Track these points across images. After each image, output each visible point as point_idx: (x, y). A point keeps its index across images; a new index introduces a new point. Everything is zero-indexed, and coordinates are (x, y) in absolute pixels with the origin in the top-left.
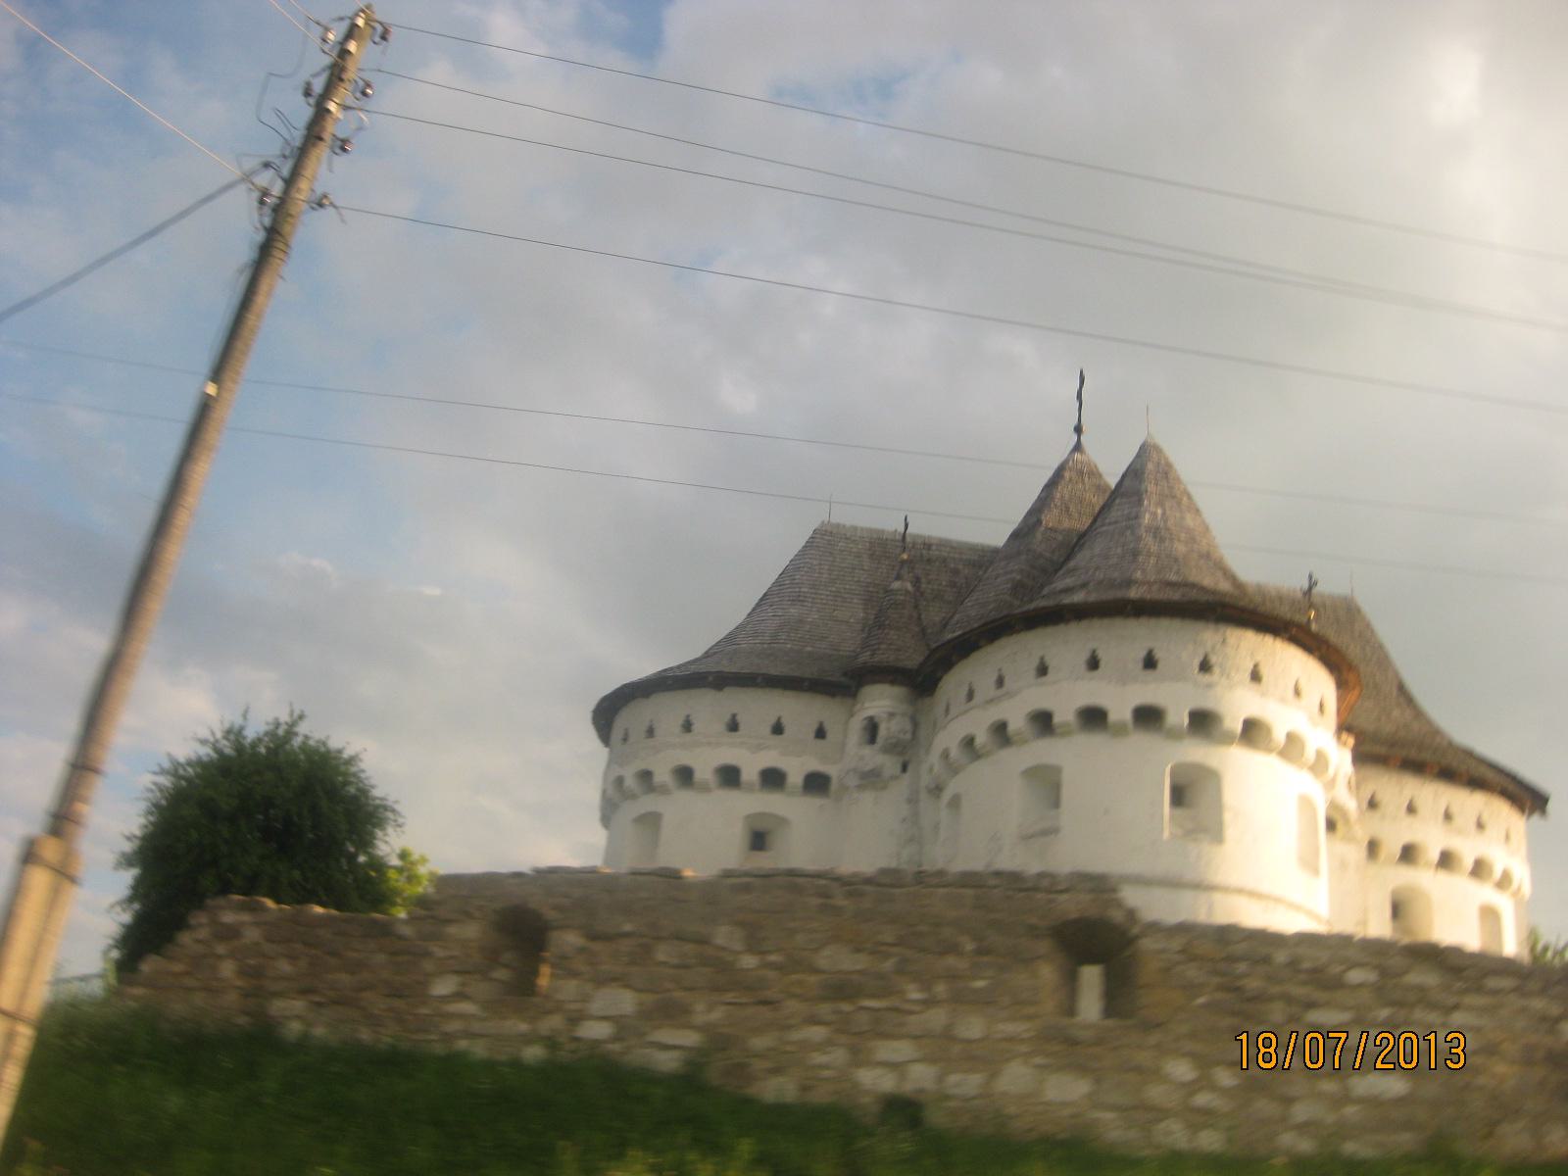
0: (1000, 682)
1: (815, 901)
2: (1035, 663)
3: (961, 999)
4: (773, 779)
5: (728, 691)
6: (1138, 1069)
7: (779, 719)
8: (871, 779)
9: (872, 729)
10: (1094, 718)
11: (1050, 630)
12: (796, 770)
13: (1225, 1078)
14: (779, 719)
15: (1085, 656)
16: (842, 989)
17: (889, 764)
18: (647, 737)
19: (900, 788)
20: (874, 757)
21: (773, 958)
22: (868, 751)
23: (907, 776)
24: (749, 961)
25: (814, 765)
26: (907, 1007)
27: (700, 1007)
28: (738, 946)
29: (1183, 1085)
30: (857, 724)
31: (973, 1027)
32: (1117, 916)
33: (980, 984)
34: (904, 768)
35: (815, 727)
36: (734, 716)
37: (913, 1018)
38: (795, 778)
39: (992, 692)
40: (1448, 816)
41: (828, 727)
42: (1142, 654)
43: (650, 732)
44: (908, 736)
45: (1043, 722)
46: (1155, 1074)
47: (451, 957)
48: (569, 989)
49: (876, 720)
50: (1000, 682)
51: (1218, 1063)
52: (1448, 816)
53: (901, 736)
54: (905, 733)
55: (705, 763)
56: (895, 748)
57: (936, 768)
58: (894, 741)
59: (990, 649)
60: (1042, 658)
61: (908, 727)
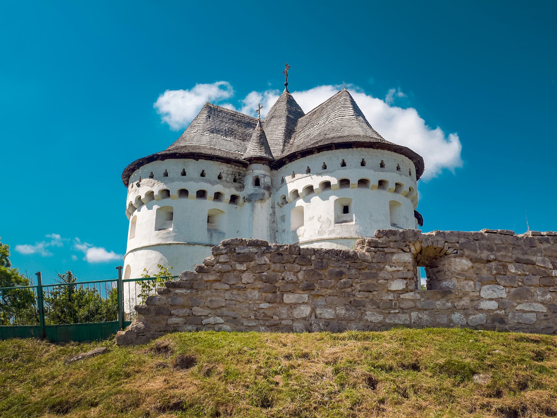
2: (341, 161)
4: (218, 196)
10: (363, 182)
11: (346, 150)
12: (228, 192)
15: (361, 161)
17: (267, 193)
19: (268, 203)
23: (271, 198)
36: (203, 171)
44: (270, 184)
47: (398, 271)
56: (268, 188)
59: (317, 154)
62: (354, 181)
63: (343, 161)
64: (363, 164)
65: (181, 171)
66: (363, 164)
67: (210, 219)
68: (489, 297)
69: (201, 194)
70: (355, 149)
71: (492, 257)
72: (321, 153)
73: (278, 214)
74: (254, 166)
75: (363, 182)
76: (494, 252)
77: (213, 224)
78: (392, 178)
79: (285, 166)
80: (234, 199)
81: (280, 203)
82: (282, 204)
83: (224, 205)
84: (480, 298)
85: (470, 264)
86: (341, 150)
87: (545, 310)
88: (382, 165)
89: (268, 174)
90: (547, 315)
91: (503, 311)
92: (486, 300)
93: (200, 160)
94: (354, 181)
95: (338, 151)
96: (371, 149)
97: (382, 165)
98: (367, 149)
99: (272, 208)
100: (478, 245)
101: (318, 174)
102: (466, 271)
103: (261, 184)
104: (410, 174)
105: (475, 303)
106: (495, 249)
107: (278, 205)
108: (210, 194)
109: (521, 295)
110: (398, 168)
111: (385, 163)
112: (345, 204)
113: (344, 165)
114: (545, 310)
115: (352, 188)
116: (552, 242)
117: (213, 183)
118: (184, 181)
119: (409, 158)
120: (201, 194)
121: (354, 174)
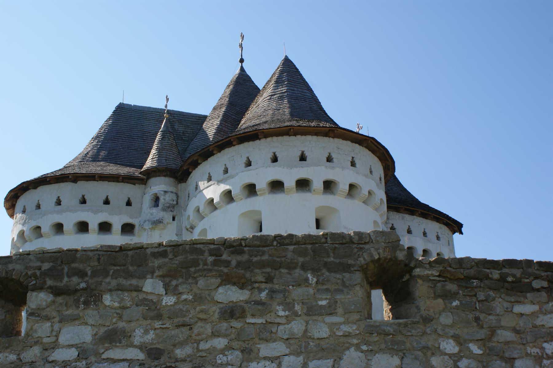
0: (226, 171)
1: (211, 259)
2: (244, 160)
3: (312, 311)
5: (79, 183)
6: (425, 348)
7: (107, 197)
9: (156, 200)
10: (277, 186)
13: (475, 349)
14: (107, 197)
15: (270, 155)
16: (232, 312)
17: (167, 217)
18: (36, 209)
20: (157, 213)
21: (184, 297)
22: (154, 210)
23: (175, 222)
24: (169, 300)
26: (278, 320)
27: (138, 332)
28: (162, 291)
29: (451, 356)
30: (148, 199)
31: (321, 330)
32: (401, 256)
33: (323, 303)
34: (174, 219)
35: (126, 200)
37: (281, 327)
39: (222, 176)
40: (425, 234)
41: (132, 200)
42: (299, 153)
43: (38, 207)
44: (175, 203)
45: (251, 189)
46: (437, 351)
48: (43, 330)
49: (158, 195)
50: (226, 171)
51: (471, 341)
52: (425, 234)
53: (171, 202)
54: (173, 201)
57: (191, 218)
58: (168, 205)
59: (219, 155)
60: (248, 158)
61: (175, 198)
62: (262, 184)
64: (275, 159)
65: (55, 200)
66: (275, 159)
68: (67, 343)
70: (263, 140)
71: (83, 285)
72: (222, 152)
75: (277, 186)
76: (87, 279)
78: (317, 174)
81: (188, 227)
84: (55, 346)
85: (51, 297)
86: (246, 144)
87: (141, 356)
88: (303, 158)
90: (144, 364)
91: (84, 362)
92: (63, 347)
93: (79, 183)
94: (262, 184)
95: (241, 146)
96: (286, 138)
97: (303, 158)
98: (280, 138)
100: (66, 270)
101: (219, 182)
102: (44, 309)
103: (160, 205)
104: (353, 164)
105: (47, 353)
106: (89, 273)
107: (187, 229)
108: (93, 226)
109: (113, 337)
110: (329, 159)
111: (307, 154)
113: (249, 164)
114: (141, 356)
115: (261, 195)
116: (171, 256)
117: (96, 212)
119: (352, 142)
121: (262, 176)
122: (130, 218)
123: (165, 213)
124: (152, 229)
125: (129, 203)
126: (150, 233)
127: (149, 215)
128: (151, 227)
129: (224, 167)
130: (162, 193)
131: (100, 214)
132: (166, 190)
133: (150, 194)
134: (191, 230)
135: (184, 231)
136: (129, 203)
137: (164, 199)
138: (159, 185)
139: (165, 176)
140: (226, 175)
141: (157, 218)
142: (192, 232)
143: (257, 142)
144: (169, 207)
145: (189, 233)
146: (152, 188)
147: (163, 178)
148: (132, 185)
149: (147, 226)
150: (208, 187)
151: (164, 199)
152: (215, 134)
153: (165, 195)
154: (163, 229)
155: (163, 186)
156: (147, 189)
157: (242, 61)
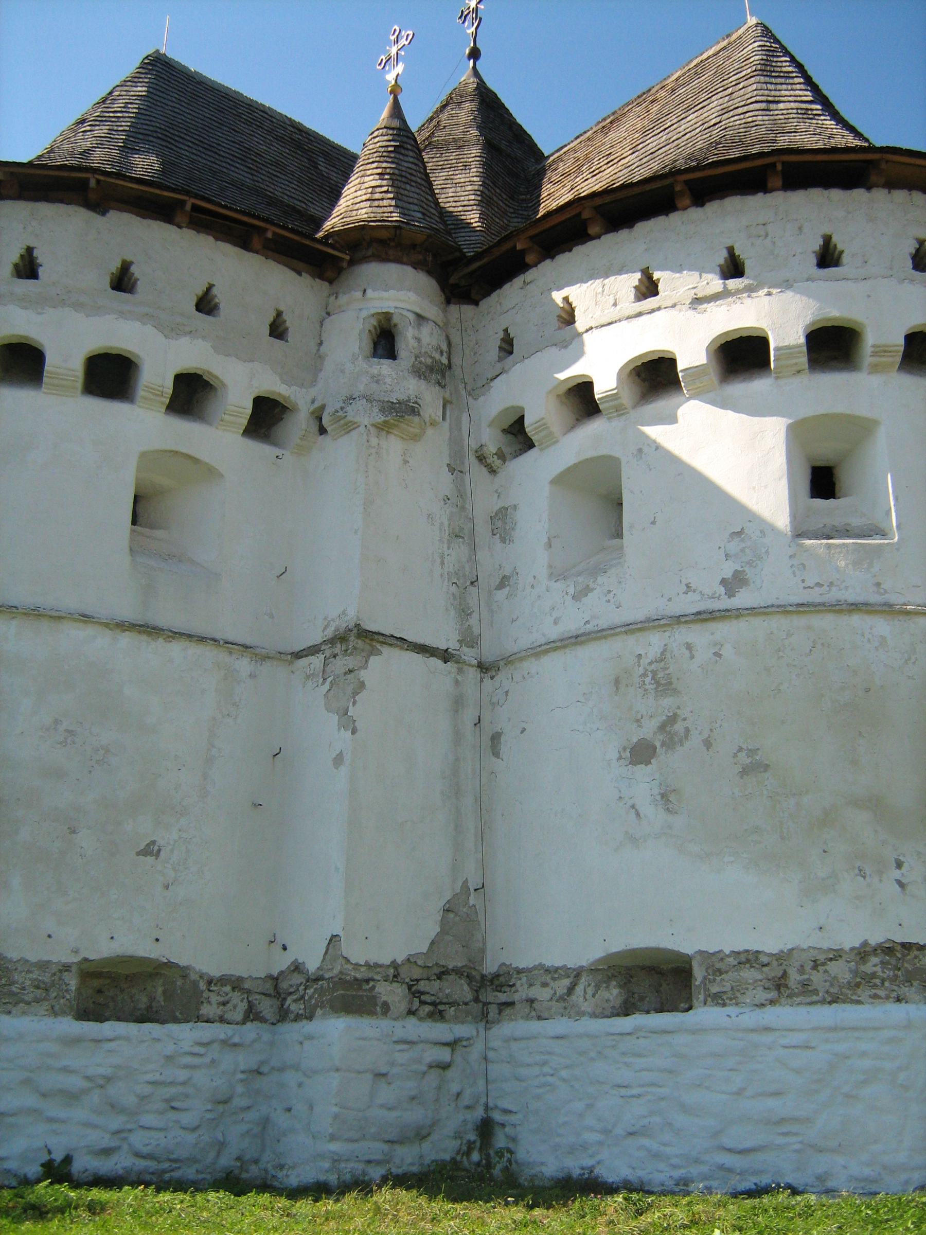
2: (817, 244)
4: (191, 394)
7: (210, 287)
8: (401, 412)
9: (384, 341)
11: (836, 194)
14: (210, 287)
17: (429, 397)
20: (395, 379)
22: (385, 367)
23: (446, 425)
25: (271, 384)
38: (237, 400)
41: (290, 320)
44: (445, 361)
49: (396, 319)
53: (437, 356)
55: (68, 344)
56: (438, 371)
58: (429, 361)
59: (695, 213)
61: (444, 347)
63: (827, 240)
67: (142, 509)
69: (110, 375)
70: (880, 194)
72: (713, 208)
73: (484, 501)
74: (373, 271)
77: (159, 533)
79: (518, 281)
80: (266, 417)
82: (501, 456)
83: (219, 440)
86: (816, 194)
89: (432, 311)
99: (452, 470)
107: (481, 458)
112: (825, 452)
117: (173, 331)
118: (25, 302)
120: (110, 375)
122: (284, 382)
123: (423, 384)
124: (383, 428)
125: (277, 330)
126: (374, 441)
127: (365, 379)
128: (380, 418)
129: (725, 254)
130: (411, 317)
131: (185, 341)
132: (418, 310)
133: (364, 314)
134: (497, 462)
135: (471, 461)
136: (277, 330)
137: (419, 340)
138: (396, 291)
139: (416, 265)
140: (651, 302)
141: (402, 397)
142: (493, 471)
143: (859, 194)
144: (431, 369)
145: (484, 471)
146: (370, 293)
147: (409, 270)
148: (293, 274)
149: (365, 416)
150: (640, 314)
151: (419, 340)
152: (486, 201)
153: (419, 325)
154: (415, 438)
155: (412, 296)
156: (343, 299)
157: (475, 54)
